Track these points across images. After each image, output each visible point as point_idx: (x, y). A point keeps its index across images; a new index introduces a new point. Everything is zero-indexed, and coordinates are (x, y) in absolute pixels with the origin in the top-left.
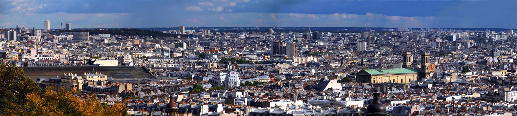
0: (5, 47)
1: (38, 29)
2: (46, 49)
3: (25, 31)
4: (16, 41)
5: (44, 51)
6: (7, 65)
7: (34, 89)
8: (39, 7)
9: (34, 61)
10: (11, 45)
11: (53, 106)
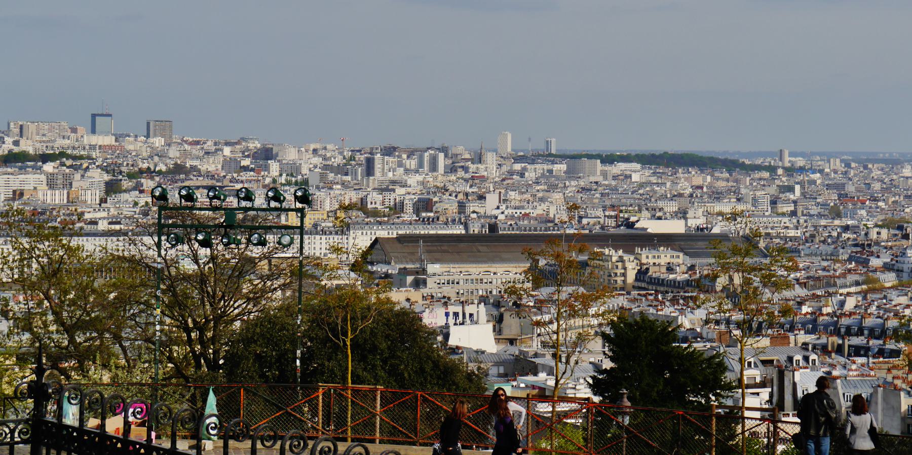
10: (435, 184)
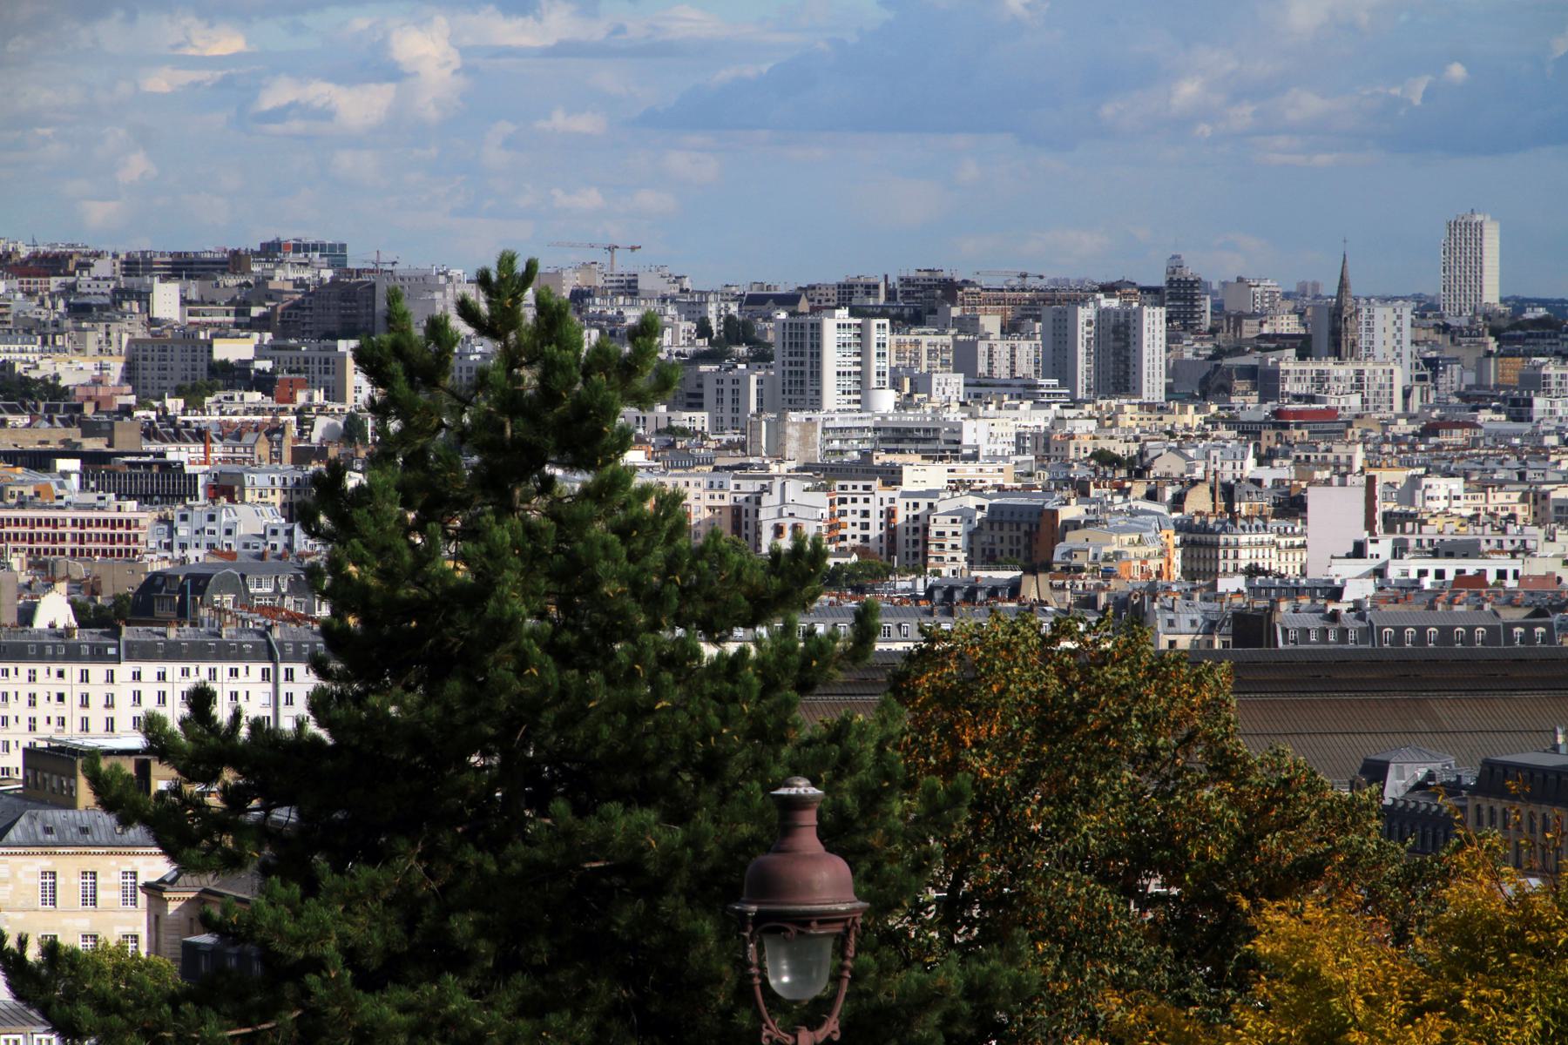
0: (1042, 461)
1: (1385, 300)
2: (1457, 485)
3: (1253, 316)
4: (1161, 409)
5: (1442, 504)
6: (1068, 633)
7: (1328, 854)
8: (1396, 91)
9: (1336, 593)
11: (1510, 1010)
